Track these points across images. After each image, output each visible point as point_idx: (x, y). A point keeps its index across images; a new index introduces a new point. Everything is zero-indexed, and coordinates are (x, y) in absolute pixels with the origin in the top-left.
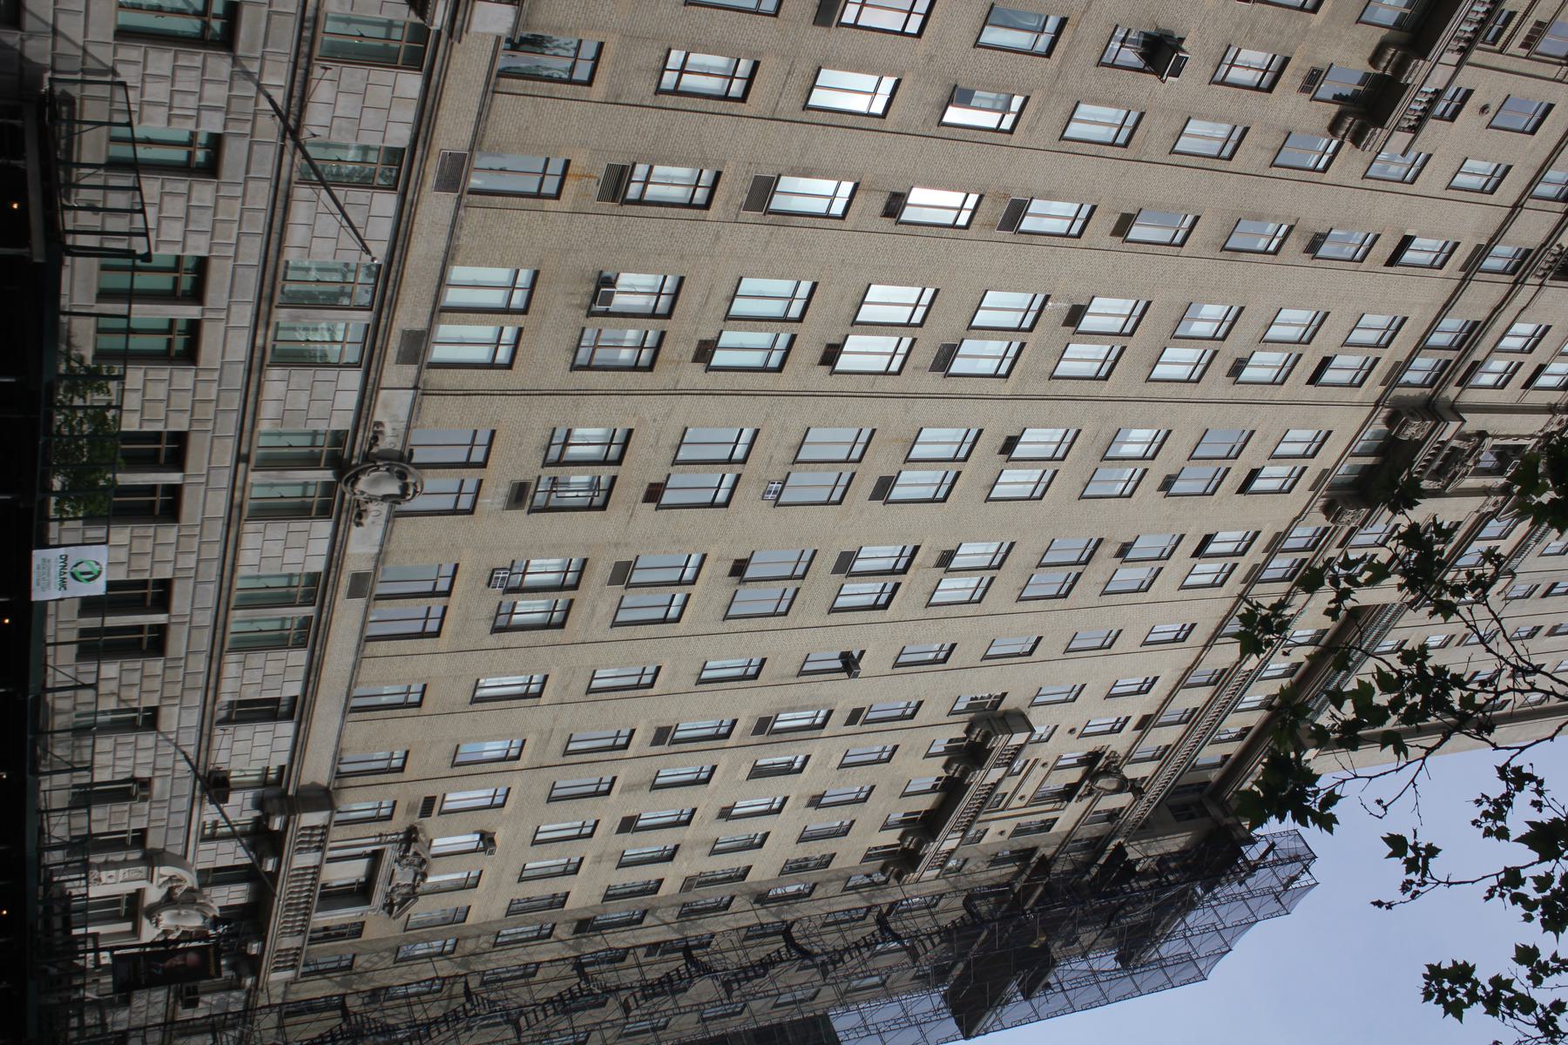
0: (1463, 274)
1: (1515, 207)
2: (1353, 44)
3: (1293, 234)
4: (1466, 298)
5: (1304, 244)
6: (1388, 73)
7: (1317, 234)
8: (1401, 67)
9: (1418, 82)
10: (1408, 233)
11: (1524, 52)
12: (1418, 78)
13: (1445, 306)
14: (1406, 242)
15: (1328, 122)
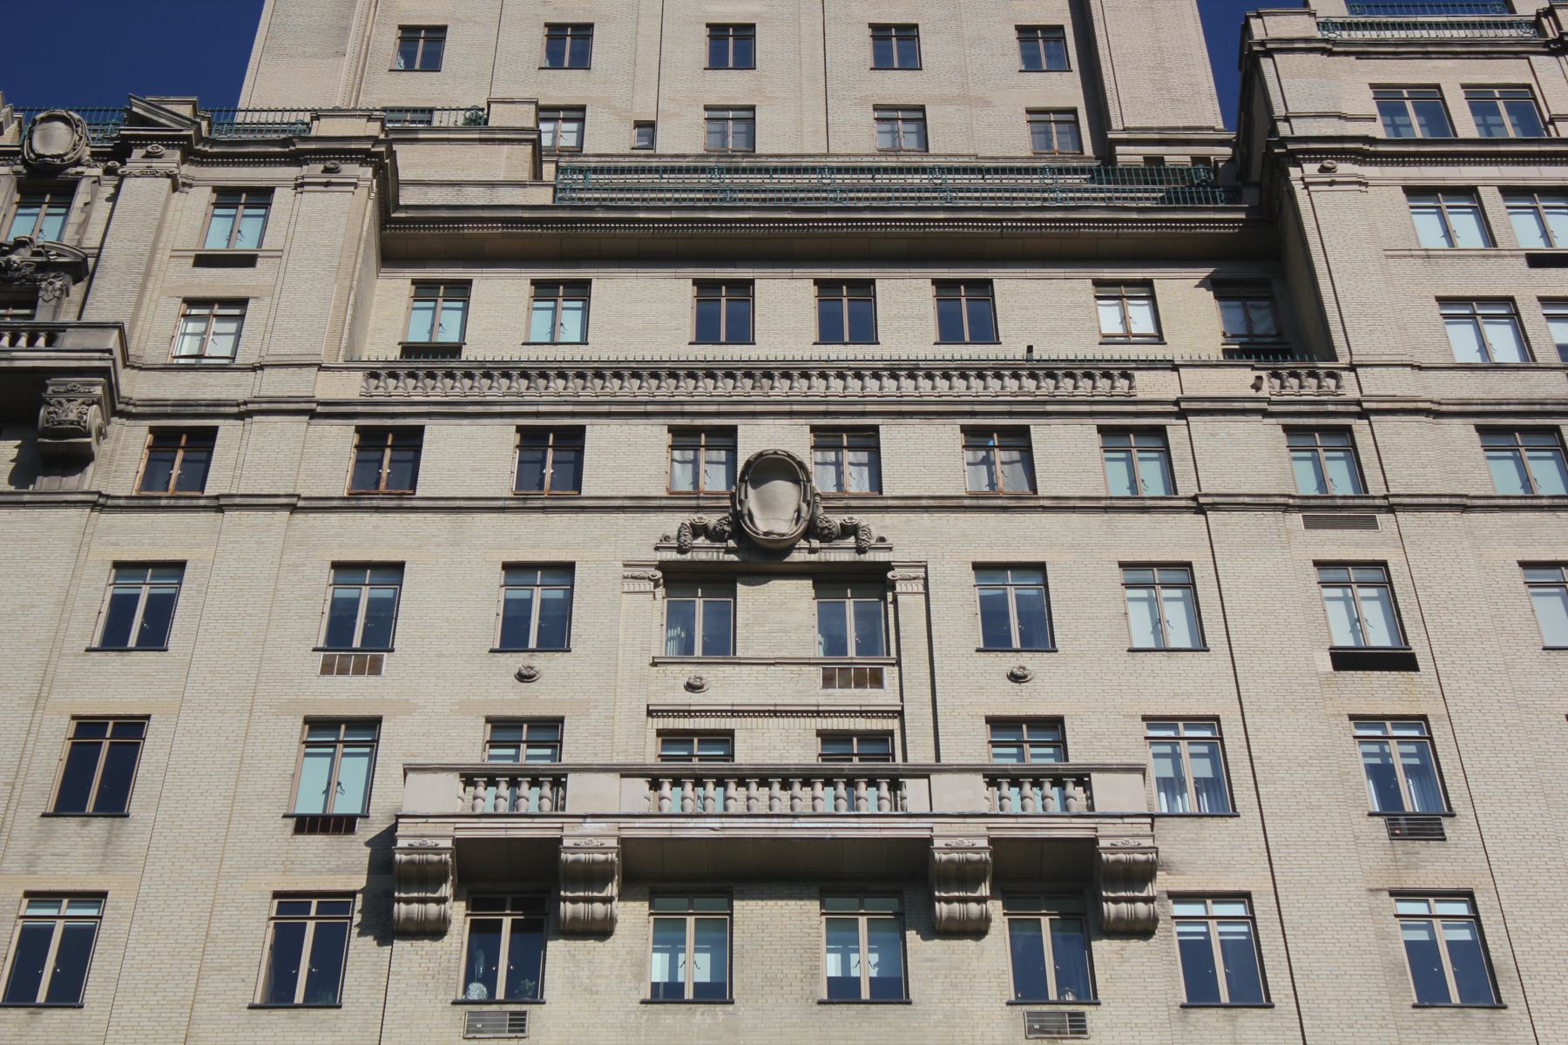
0: (1381, 518)
1: (1200, 510)
2: (954, 985)
3: (1410, 883)
4: (1434, 482)
5: (1425, 850)
6: (984, 890)
7: (1393, 836)
8: (963, 876)
9: (979, 827)
10: (1326, 663)
11: (890, 674)
12: (1136, 830)
13: (1465, 509)
14: (1345, 660)
15: (1135, 945)
